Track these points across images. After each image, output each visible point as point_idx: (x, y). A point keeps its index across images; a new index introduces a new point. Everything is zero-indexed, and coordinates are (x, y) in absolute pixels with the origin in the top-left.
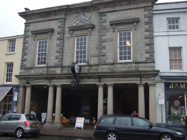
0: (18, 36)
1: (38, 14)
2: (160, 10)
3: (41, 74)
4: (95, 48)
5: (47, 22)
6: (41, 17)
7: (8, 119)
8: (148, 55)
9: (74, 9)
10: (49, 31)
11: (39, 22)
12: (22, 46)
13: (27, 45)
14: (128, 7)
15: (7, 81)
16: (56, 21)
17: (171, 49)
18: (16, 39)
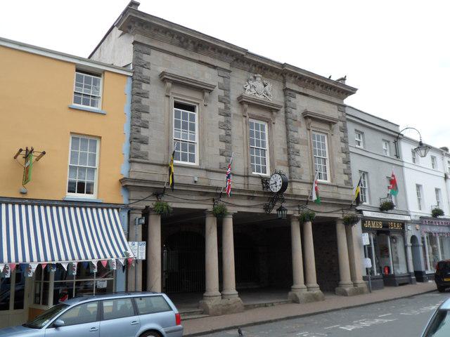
0: (112, 66)
1: (179, 38)
2: (356, 118)
3: (195, 185)
4: (282, 150)
5: (195, 65)
6: (181, 45)
7: (220, 313)
8: (223, 159)
9: (249, 62)
10: (169, 79)
11: (175, 55)
12: (128, 98)
13: (144, 101)
14: (319, 95)
15: (71, 190)
16: (214, 72)
17: (76, 137)
18: (106, 73)
